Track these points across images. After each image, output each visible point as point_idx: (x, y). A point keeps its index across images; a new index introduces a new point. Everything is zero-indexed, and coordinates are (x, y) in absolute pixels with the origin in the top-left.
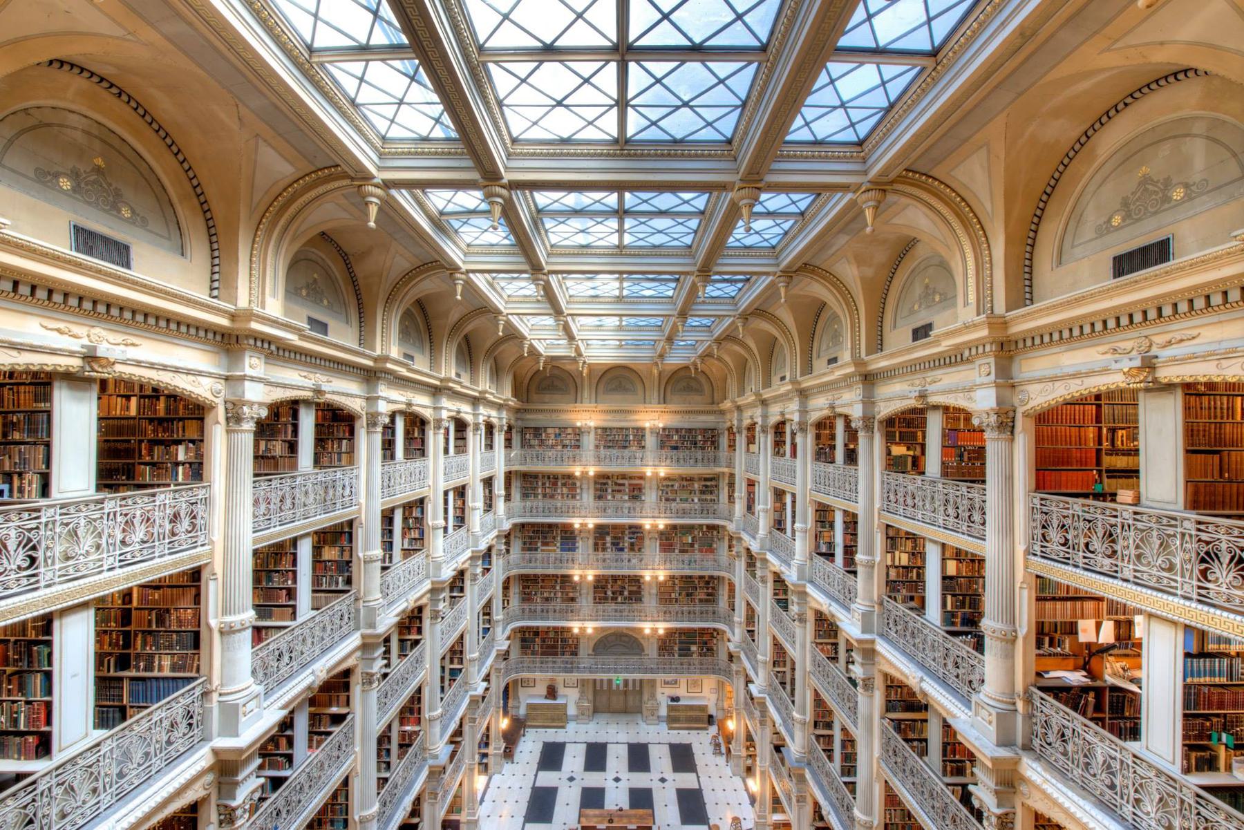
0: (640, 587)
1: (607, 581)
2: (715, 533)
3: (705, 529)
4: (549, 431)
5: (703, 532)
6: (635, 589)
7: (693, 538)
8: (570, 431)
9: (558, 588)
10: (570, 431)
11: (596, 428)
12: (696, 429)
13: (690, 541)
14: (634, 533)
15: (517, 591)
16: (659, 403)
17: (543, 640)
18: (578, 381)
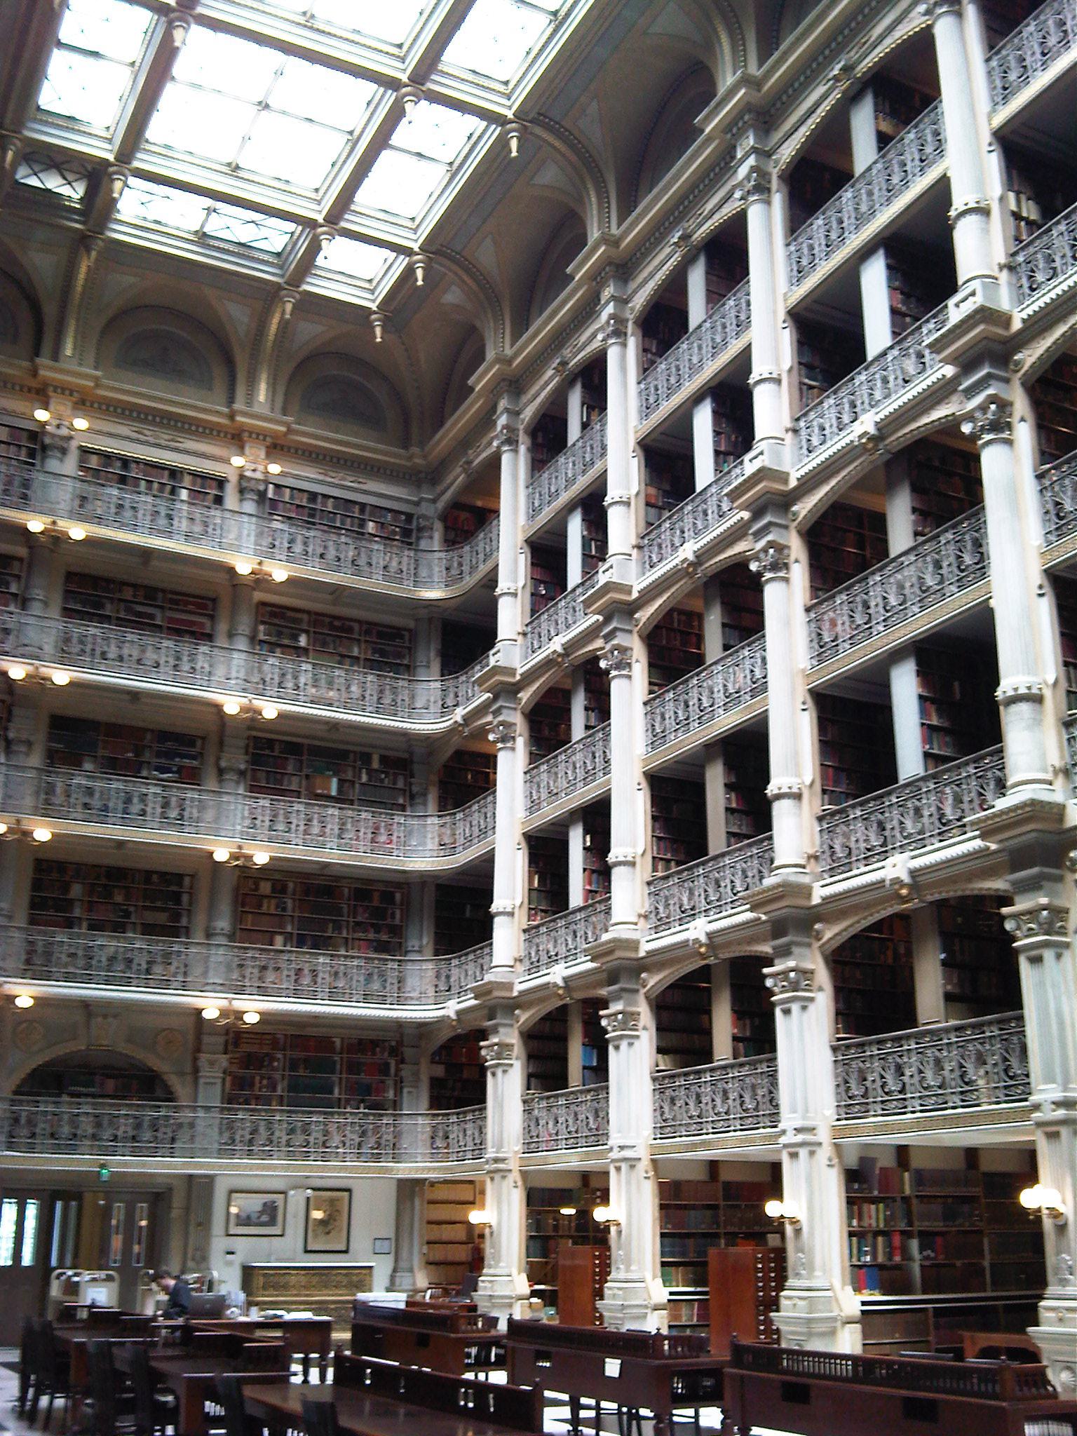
0: (176, 916)
2: (400, 784)
3: (375, 764)
6: (162, 918)
7: (341, 782)
11: (85, 451)
12: (363, 506)
13: (334, 793)
14: (169, 755)
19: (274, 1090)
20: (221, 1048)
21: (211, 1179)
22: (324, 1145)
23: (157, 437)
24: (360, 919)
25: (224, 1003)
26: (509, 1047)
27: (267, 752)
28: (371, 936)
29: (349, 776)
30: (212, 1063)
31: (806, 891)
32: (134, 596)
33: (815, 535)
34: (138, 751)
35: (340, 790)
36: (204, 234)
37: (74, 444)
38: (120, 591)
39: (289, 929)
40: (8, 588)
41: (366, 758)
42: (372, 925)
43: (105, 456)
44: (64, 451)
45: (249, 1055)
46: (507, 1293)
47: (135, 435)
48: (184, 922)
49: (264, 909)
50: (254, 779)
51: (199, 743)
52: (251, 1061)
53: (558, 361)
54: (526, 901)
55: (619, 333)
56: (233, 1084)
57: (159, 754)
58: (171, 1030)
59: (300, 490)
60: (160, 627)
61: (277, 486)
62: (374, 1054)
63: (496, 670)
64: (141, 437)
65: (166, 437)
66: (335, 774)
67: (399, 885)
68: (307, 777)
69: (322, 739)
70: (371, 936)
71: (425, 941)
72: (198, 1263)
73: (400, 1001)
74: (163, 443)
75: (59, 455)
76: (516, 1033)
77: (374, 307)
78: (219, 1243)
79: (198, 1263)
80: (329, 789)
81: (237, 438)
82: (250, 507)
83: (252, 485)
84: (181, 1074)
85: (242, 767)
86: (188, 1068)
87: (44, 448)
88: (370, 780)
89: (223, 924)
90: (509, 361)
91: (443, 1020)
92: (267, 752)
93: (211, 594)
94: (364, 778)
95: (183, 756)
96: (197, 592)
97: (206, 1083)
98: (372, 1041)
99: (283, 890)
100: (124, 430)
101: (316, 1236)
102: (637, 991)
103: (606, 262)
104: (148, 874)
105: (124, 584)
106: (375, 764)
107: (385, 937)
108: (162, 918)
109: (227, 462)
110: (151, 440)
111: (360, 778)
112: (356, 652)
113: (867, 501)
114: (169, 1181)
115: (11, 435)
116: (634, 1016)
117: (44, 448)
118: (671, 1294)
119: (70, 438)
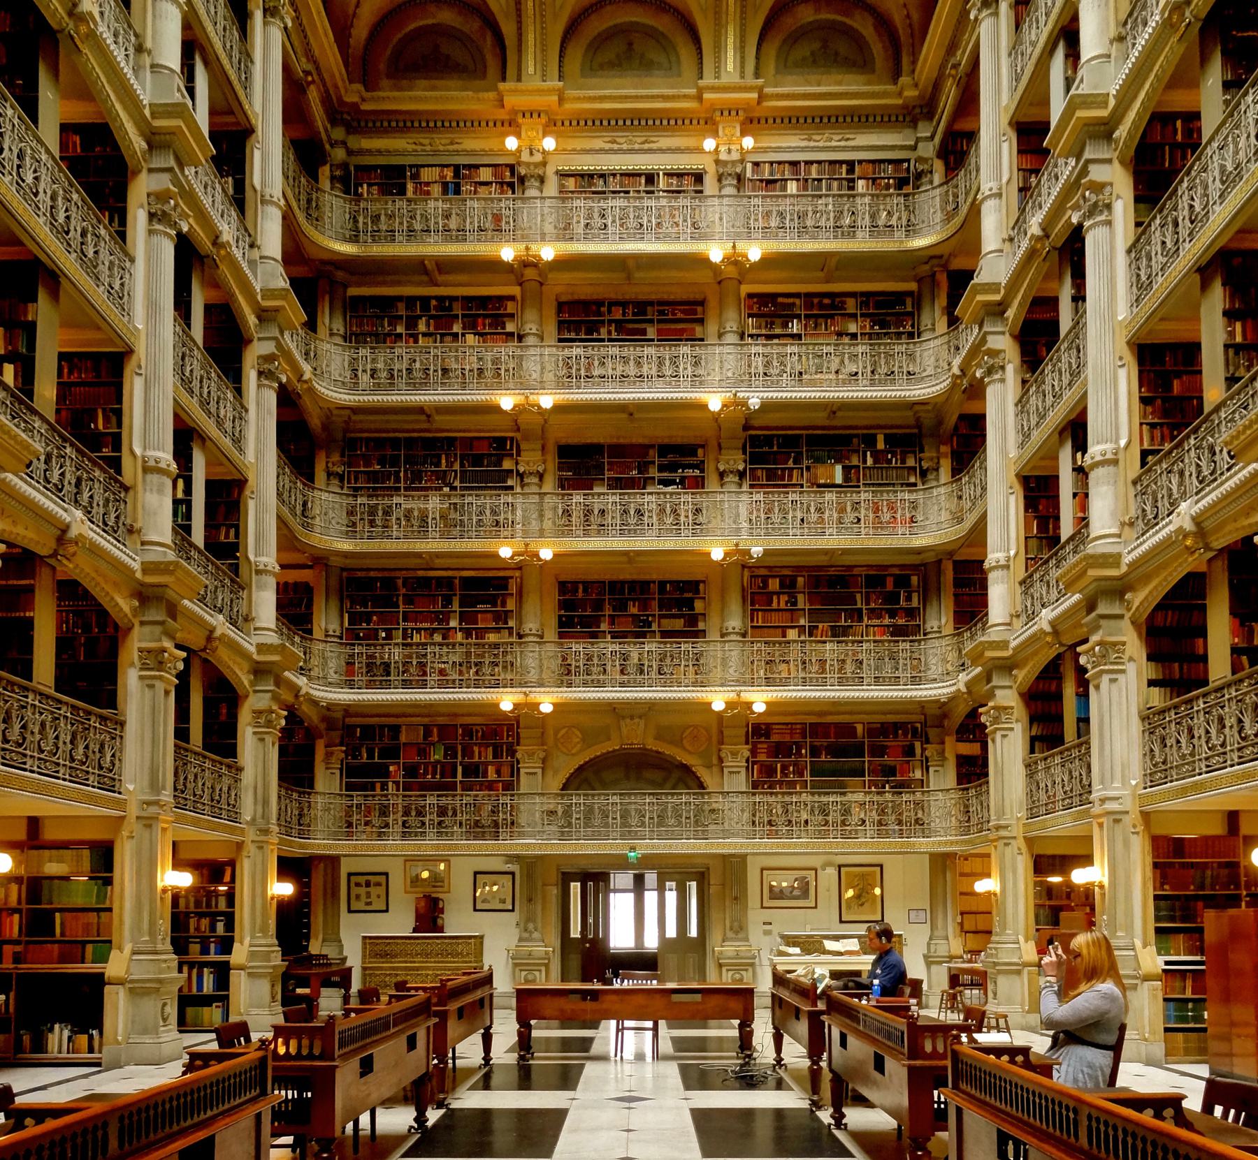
0: (693, 620)
1: (598, 606)
3: (881, 445)
4: (426, 175)
5: (877, 456)
6: (678, 624)
7: (847, 470)
8: (485, 174)
9: (453, 623)
10: (485, 174)
11: (563, 175)
12: (851, 165)
13: (839, 479)
14: (672, 468)
15: (334, 627)
17: (411, 771)
18: (508, 29)
19: (802, 775)
20: (743, 739)
21: (743, 857)
22: (843, 823)
23: (631, 142)
24: (873, 605)
25: (732, 696)
27: (766, 449)
28: (887, 621)
29: (855, 461)
30: (734, 754)
32: (624, 314)
34: (643, 468)
35: (846, 478)
37: (550, 171)
38: (610, 312)
39: (802, 622)
40: (504, 328)
41: (870, 441)
42: (888, 611)
43: (582, 176)
44: (542, 180)
45: (778, 744)
46: (1015, 960)
47: (608, 146)
48: (701, 626)
49: (775, 605)
50: (753, 477)
51: (700, 452)
52: (780, 750)
56: (760, 772)
57: (662, 469)
58: (696, 727)
59: (779, 163)
60: (653, 340)
61: (756, 164)
62: (896, 736)
64: (615, 146)
65: (639, 140)
66: (837, 462)
67: (914, 567)
68: (808, 468)
69: (823, 428)
70: (887, 621)
71: (943, 621)
72: (737, 933)
73: (916, 680)
74: (637, 146)
75: (537, 184)
78: (755, 916)
79: (737, 933)
80: (832, 476)
81: (708, 123)
83: (729, 169)
84: (709, 766)
85: (741, 467)
86: (715, 761)
87: (522, 180)
88: (875, 462)
89: (735, 622)
92: (766, 449)
93: (699, 297)
94: (870, 462)
95: (684, 467)
96: (685, 297)
97: (731, 773)
98: (895, 724)
99: (793, 584)
100: (599, 144)
101: (849, 907)
104: (662, 584)
105: (613, 304)
106: (881, 445)
107: (901, 622)
108: (678, 624)
109: (700, 150)
110: (625, 147)
111: (865, 461)
112: (853, 328)
114: (706, 861)
115: (495, 175)
117: (522, 180)
118: (1167, 963)
119: (544, 164)
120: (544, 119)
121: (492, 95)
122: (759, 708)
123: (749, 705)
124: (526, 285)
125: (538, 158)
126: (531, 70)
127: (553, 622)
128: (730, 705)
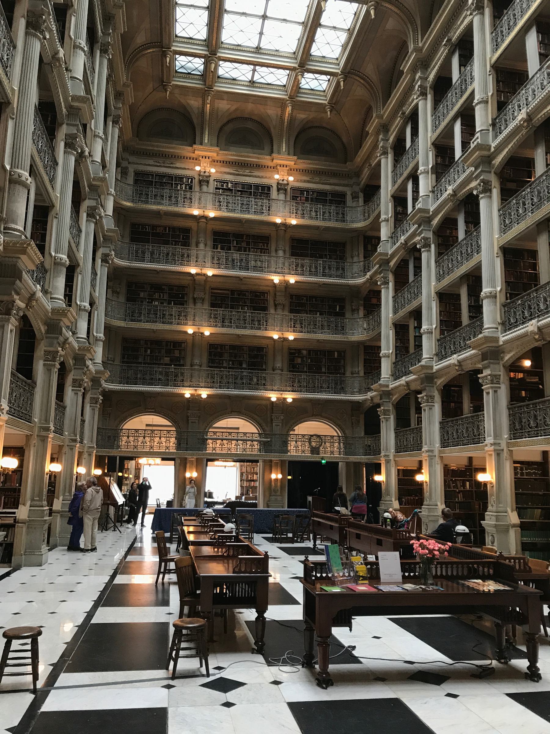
16: (289, 154)
26: (389, 410)
31: (497, 339)
33: (502, 175)
36: (254, 82)
44: (208, 182)
53: (400, 113)
54: (394, 351)
55: (423, 94)
63: (381, 254)
71: (360, 369)
76: (391, 405)
77: (326, 102)
82: (282, 197)
83: (283, 187)
90: (382, 117)
91: (366, 400)
102: (433, 386)
103: (416, 60)
113: (527, 154)
116: (432, 397)
119: (210, 176)
120: (210, 159)
121: (190, 148)
122: (290, 400)
123: (285, 399)
124: (200, 224)
125: (207, 174)
126: (206, 141)
127: (205, 360)
128: (278, 399)
